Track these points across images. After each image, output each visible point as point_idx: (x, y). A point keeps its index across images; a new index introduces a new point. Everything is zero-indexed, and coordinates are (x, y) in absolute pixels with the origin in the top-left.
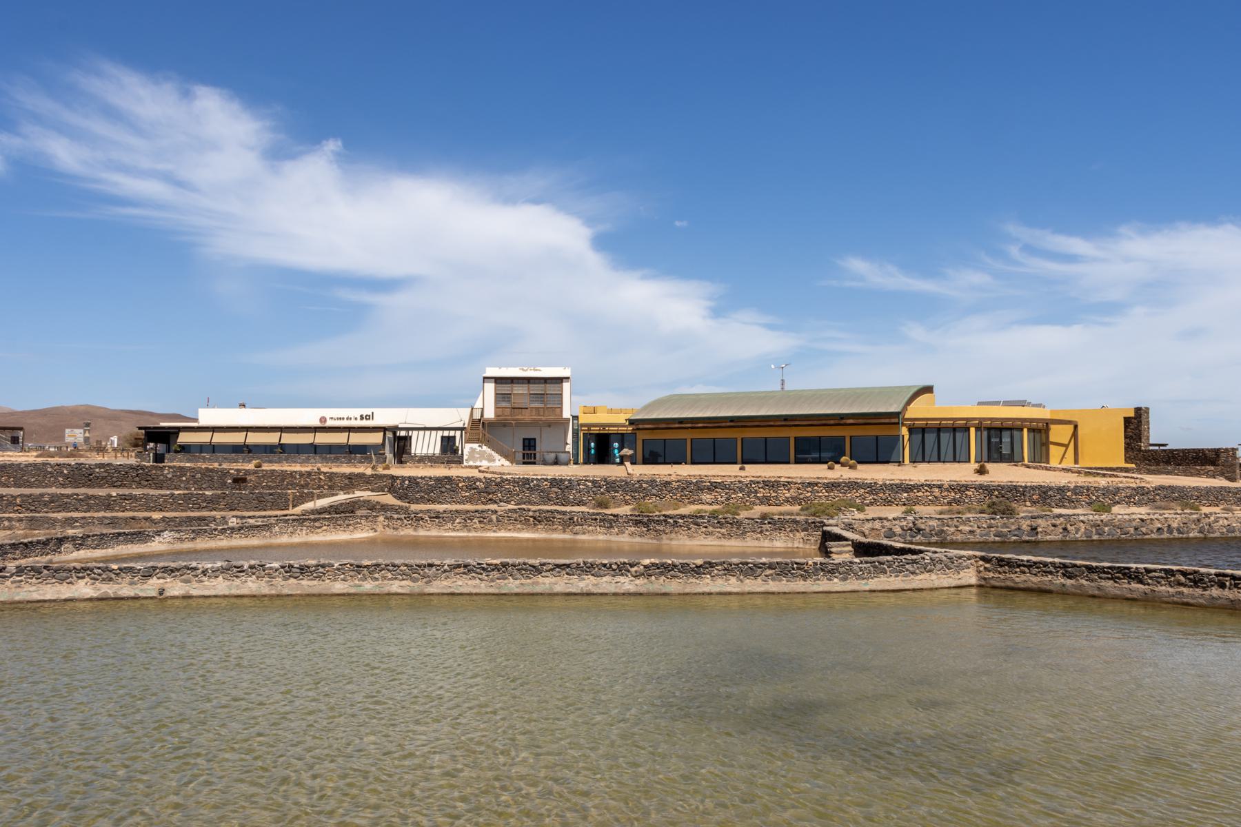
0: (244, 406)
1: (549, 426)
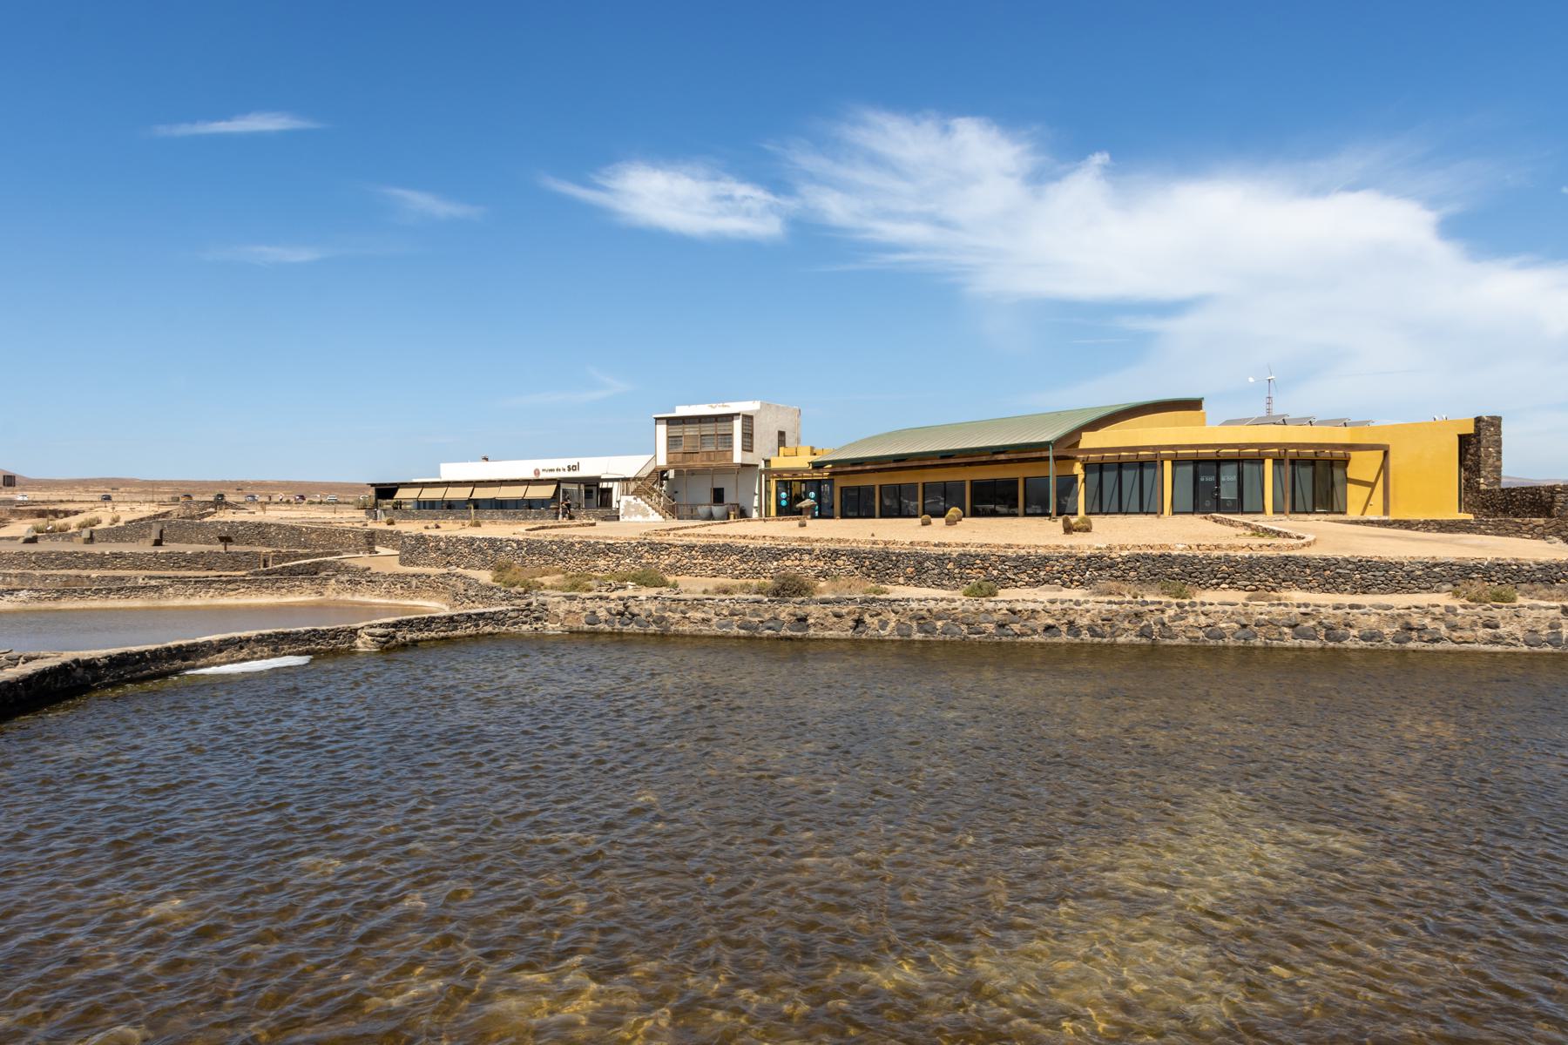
0: (486, 459)
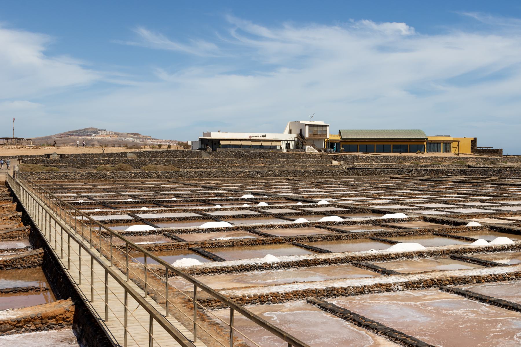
1: (318, 140)
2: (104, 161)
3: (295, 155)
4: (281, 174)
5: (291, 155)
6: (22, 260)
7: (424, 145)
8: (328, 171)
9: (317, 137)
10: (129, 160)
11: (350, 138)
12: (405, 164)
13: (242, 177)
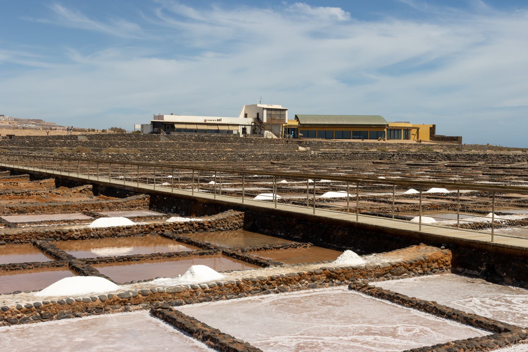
1: (276, 125)
2: (59, 144)
3: (258, 140)
4: (263, 158)
5: (254, 140)
6: (224, 222)
7: (385, 132)
8: (311, 156)
9: (275, 122)
10: (88, 143)
11: (309, 123)
12: (371, 150)
13: (224, 160)
